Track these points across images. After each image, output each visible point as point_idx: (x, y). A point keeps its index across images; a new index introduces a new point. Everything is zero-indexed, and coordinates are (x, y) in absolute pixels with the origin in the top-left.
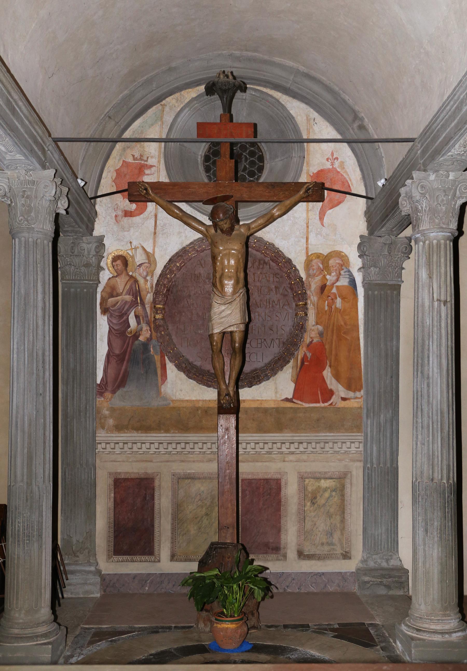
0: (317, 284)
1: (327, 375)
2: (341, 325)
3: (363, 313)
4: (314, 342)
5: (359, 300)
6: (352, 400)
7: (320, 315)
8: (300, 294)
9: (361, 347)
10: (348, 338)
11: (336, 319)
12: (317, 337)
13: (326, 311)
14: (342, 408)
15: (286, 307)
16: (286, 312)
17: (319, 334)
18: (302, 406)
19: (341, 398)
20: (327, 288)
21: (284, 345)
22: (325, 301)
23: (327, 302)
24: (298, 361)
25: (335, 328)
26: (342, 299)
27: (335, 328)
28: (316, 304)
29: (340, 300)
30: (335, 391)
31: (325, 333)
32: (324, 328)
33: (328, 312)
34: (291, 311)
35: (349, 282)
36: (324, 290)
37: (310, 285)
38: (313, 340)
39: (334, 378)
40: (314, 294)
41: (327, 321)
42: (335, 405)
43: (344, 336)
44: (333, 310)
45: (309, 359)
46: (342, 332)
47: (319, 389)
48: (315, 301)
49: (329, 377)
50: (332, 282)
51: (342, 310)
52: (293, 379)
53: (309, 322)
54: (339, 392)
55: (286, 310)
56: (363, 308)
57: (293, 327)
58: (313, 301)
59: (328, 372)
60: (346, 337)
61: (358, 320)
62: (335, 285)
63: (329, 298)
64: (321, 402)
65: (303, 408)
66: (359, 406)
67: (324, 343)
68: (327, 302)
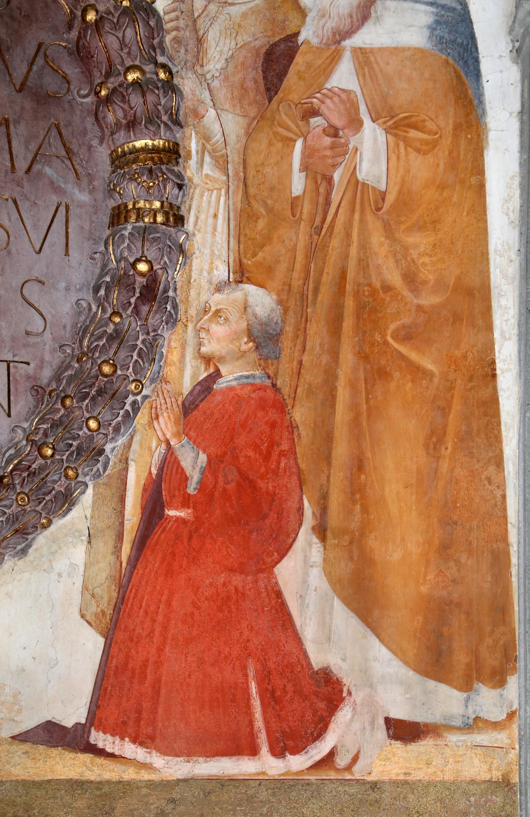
0: (244, 38)
1: (305, 582)
2: (387, 288)
3: (515, 216)
4: (220, 385)
5: (492, 136)
6: (453, 738)
7: (261, 224)
8: (135, 83)
9: (505, 417)
10: (429, 365)
11: (354, 251)
12: (243, 354)
13: (295, 202)
14: (395, 783)
15: (48, 171)
16: (55, 199)
17: (251, 337)
18: (146, 776)
19: (388, 720)
20: (299, 59)
21: (39, 401)
22: (290, 142)
23: (299, 145)
24: (122, 500)
25: (349, 303)
26: (387, 131)
27: (349, 303)
28: (234, 158)
29: (381, 136)
30: (347, 681)
31: (289, 329)
32: (280, 302)
33: (306, 208)
34: (83, 197)
35: (432, 29)
36: (282, 75)
37: (200, 41)
38: (217, 374)
39: (347, 602)
40: (222, 94)
41: (300, 258)
42: (349, 768)
43: (403, 349)
44: (335, 197)
45: (192, 489)
46: (393, 327)
47: (251, 674)
48: (232, 139)
49: (312, 599)
50: (330, 24)
51: (390, 199)
52: (93, 608)
53: (196, 263)
54: (371, 686)
55: (57, 190)
56: (517, 181)
57: (96, 289)
58: (218, 137)
59: (307, 564)
60: (414, 356)
61: (485, 255)
62: (347, 43)
63: (315, 121)
64: (264, 749)
65: (151, 785)
66: (497, 775)
67: (286, 391)
68: (299, 145)
